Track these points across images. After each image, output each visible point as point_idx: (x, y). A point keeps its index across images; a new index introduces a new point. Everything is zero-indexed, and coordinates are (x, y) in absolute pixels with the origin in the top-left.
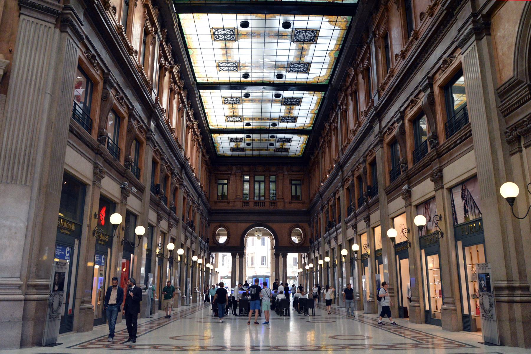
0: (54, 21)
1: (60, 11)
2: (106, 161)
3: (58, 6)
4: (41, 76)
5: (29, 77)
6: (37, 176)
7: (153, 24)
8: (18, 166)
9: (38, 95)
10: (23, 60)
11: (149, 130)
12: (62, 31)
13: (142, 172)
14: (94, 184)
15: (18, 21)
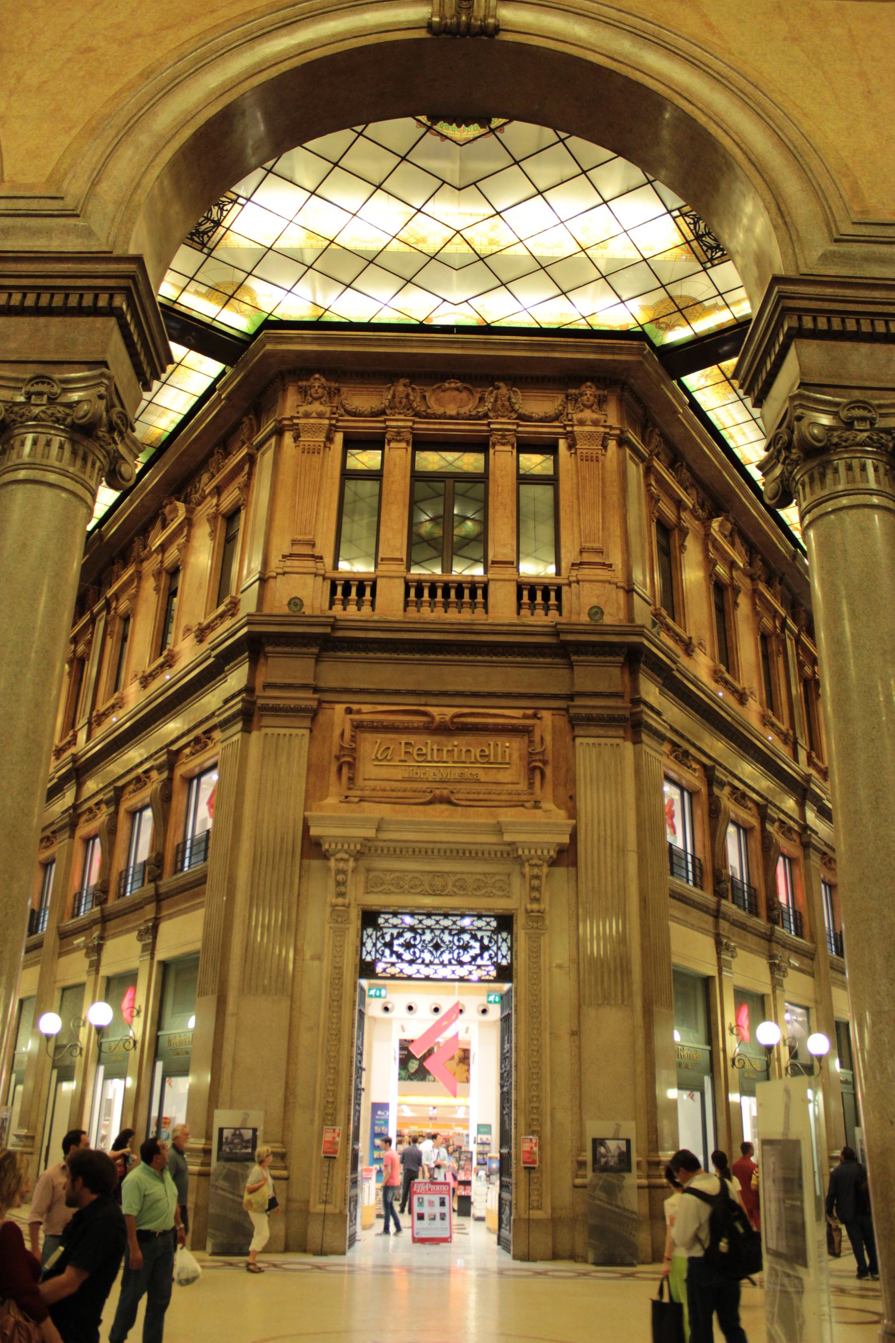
0: (621, 733)
1: (627, 714)
2: (734, 923)
3: (624, 708)
4: (618, 827)
5: (602, 833)
6: (637, 987)
7: (775, 614)
8: (609, 977)
9: (618, 858)
10: (589, 809)
11: (805, 827)
12: (634, 743)
13: (806, 919)
14: (720, 974)
15: (574, 747)
